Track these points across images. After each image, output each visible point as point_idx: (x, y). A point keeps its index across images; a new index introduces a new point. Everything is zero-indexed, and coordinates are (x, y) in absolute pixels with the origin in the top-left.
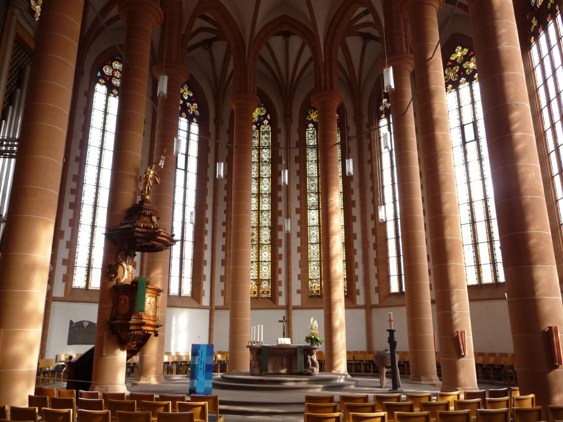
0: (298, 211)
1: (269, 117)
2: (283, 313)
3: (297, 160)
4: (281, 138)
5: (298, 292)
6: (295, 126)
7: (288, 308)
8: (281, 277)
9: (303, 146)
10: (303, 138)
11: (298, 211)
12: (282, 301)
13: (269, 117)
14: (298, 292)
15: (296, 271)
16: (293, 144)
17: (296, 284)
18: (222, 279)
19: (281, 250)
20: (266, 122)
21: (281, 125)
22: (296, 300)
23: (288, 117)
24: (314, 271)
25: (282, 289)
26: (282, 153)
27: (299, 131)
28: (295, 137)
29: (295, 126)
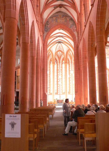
0: (61, 79)
1: (56, 62)
2: (59, 95)
3: (61, 70)
4: (58, 66)
5: (61, 92)
6: (61, 64)
7: (60, 94)
8: (59, 90)
9: (62, 67)
10: (62, 66)
11: (61, 79)
12: (59, 93)
13: (56, 62)
14: (61, 92)
15: (61, 89)
16: (60, 67)
17: (61, 91)
18: (49, 90)
19: (59, 85)
20: (56, 63)
21: (58, 64)
22: (61, 93)
23: (60, 62)
24: (64, 89)
25: (59, 92)
26: (59, 69)
27: (61, 65)
28: (61, 66)
29: (61, 64)
